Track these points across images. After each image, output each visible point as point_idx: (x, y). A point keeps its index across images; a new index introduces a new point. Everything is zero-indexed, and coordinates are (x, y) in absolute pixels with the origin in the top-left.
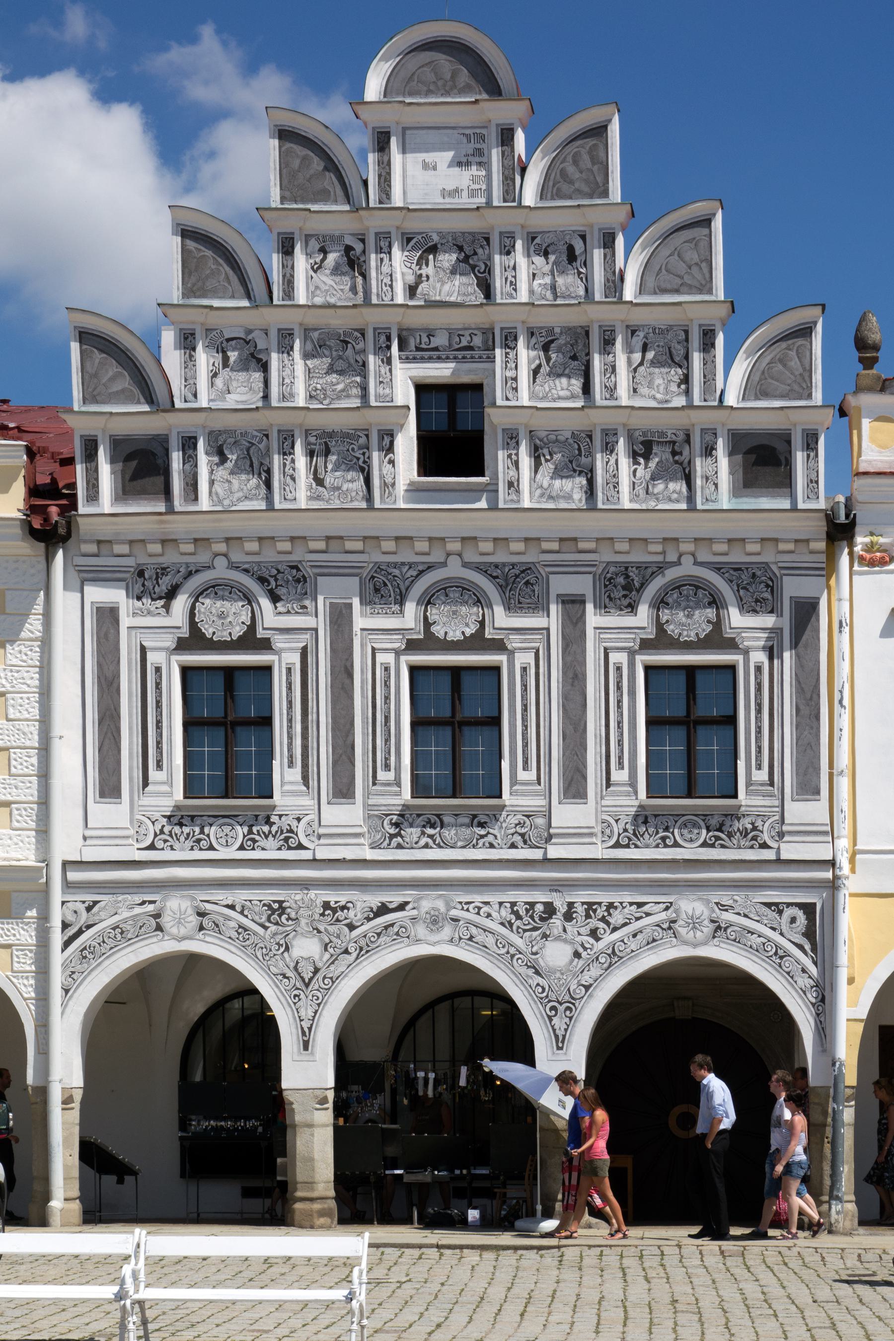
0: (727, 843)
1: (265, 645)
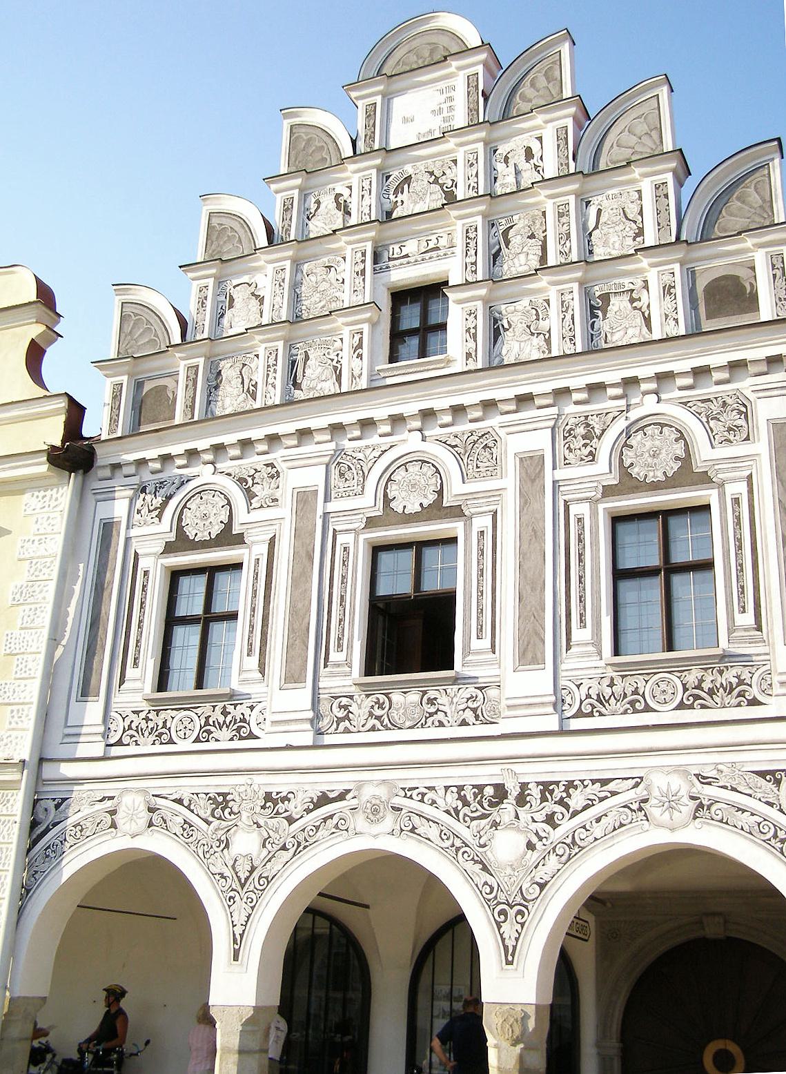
0: (709, 702)
1: (239, 540)
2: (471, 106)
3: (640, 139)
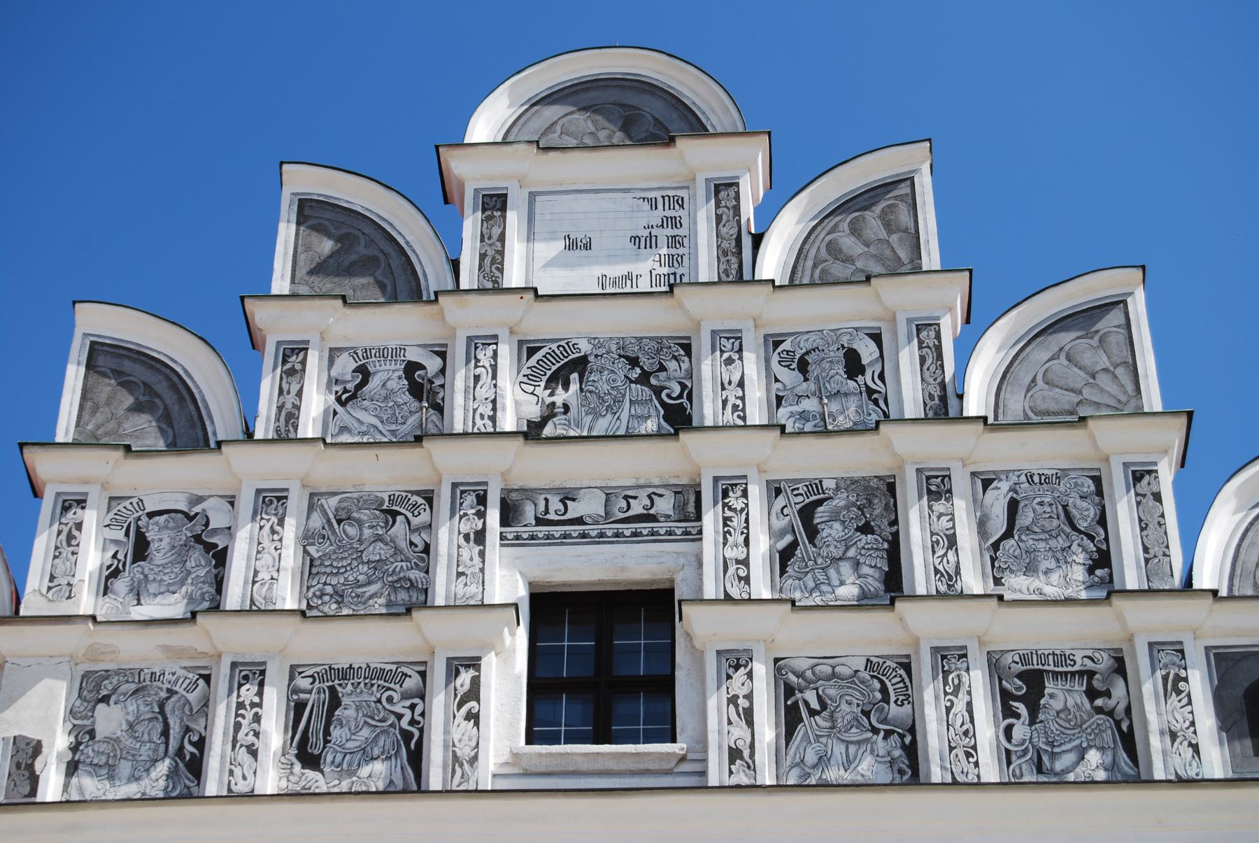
2: (725, 245)
3: (1094, 378)
